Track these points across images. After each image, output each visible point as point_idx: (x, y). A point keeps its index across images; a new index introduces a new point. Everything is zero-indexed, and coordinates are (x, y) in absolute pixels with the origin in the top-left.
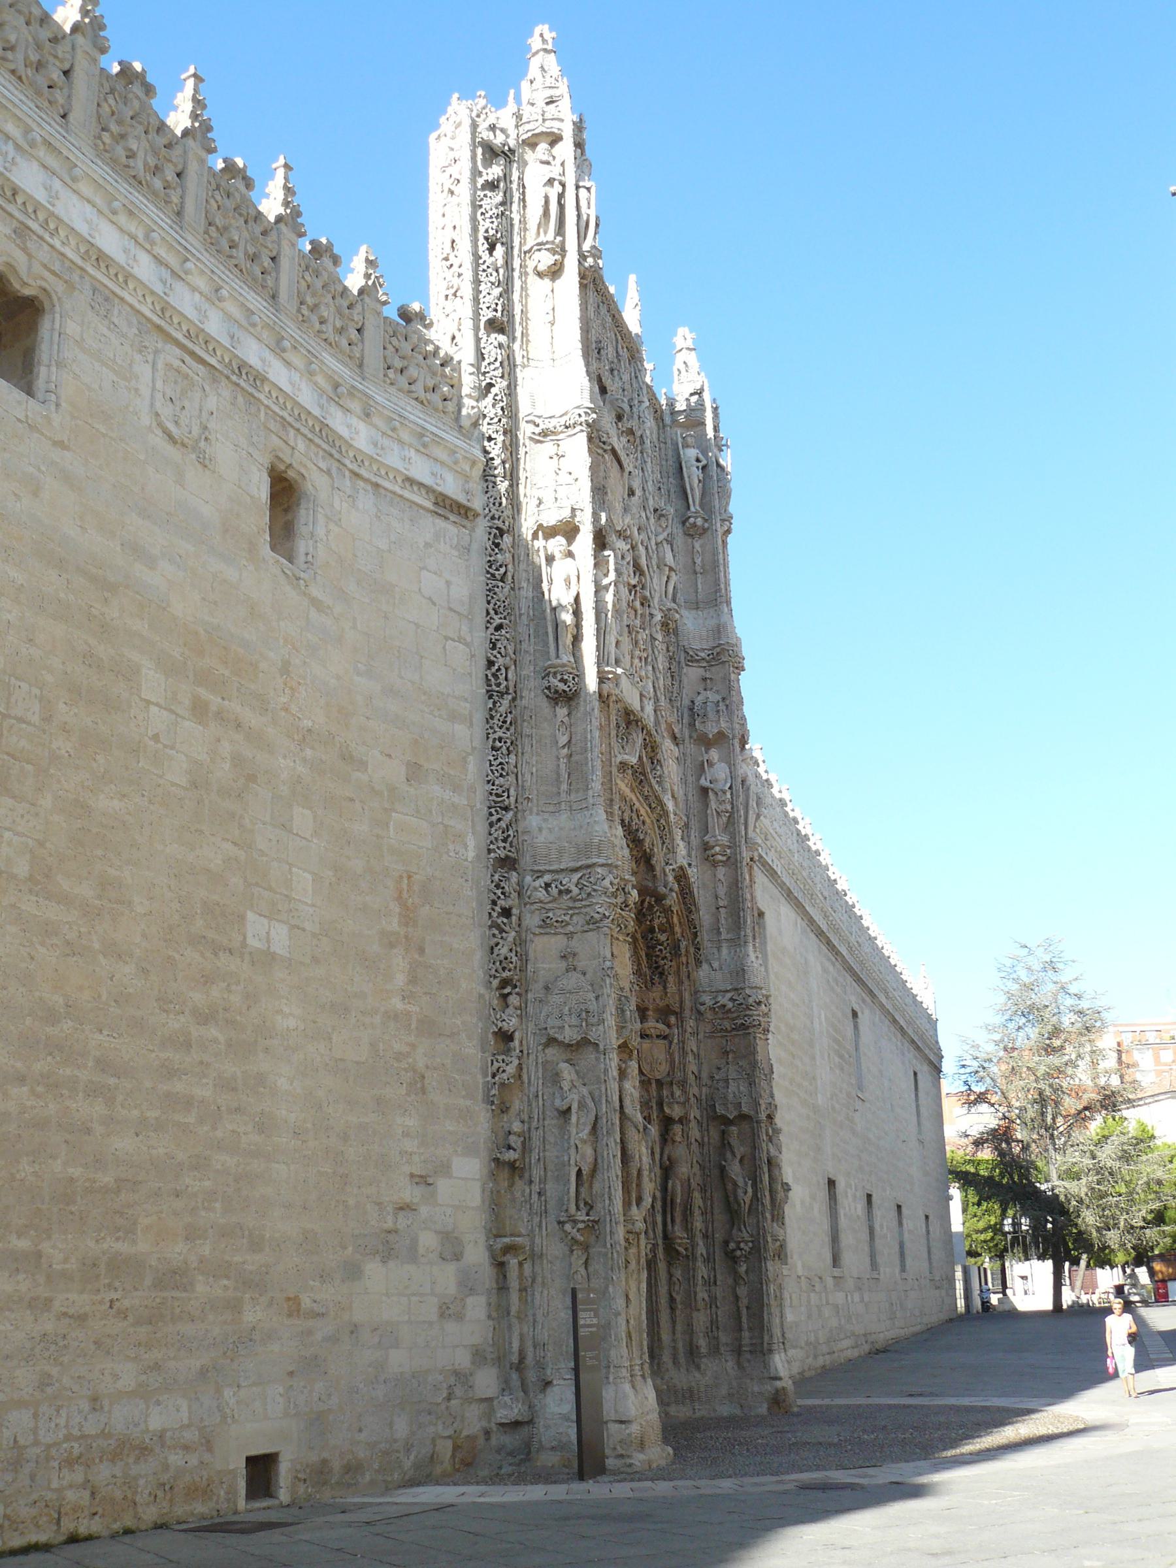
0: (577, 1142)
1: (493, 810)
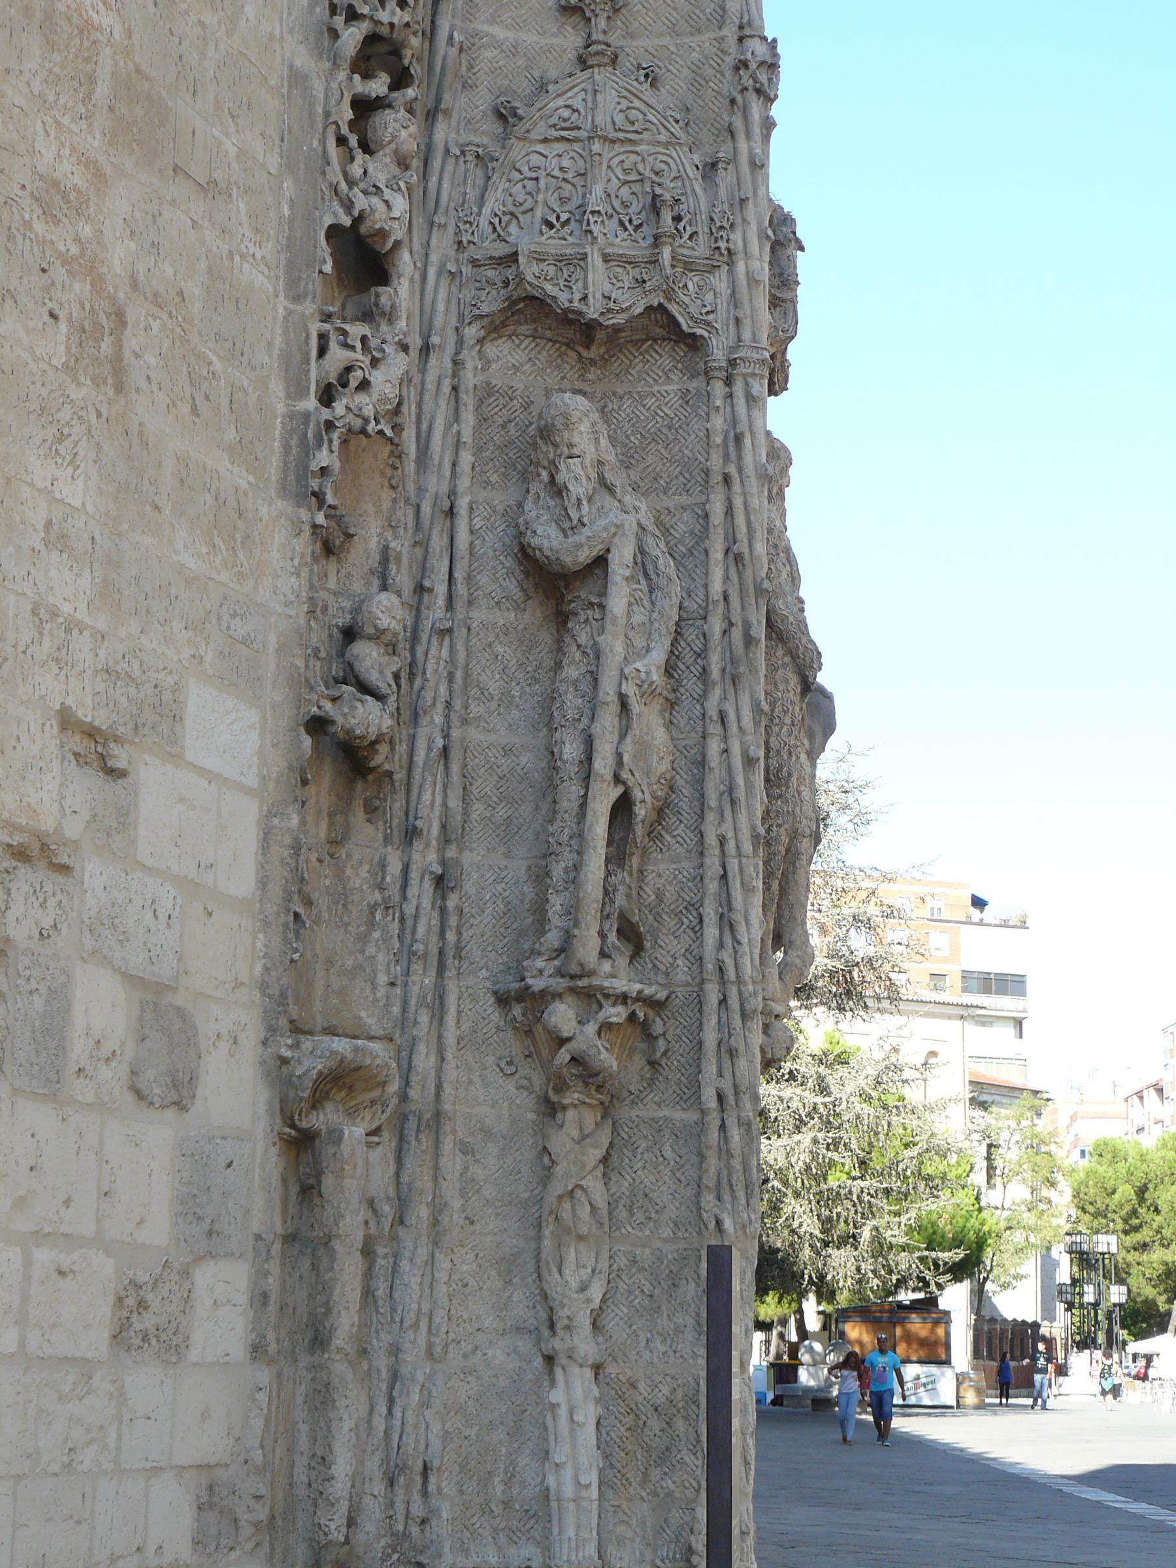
0: (630, 689)
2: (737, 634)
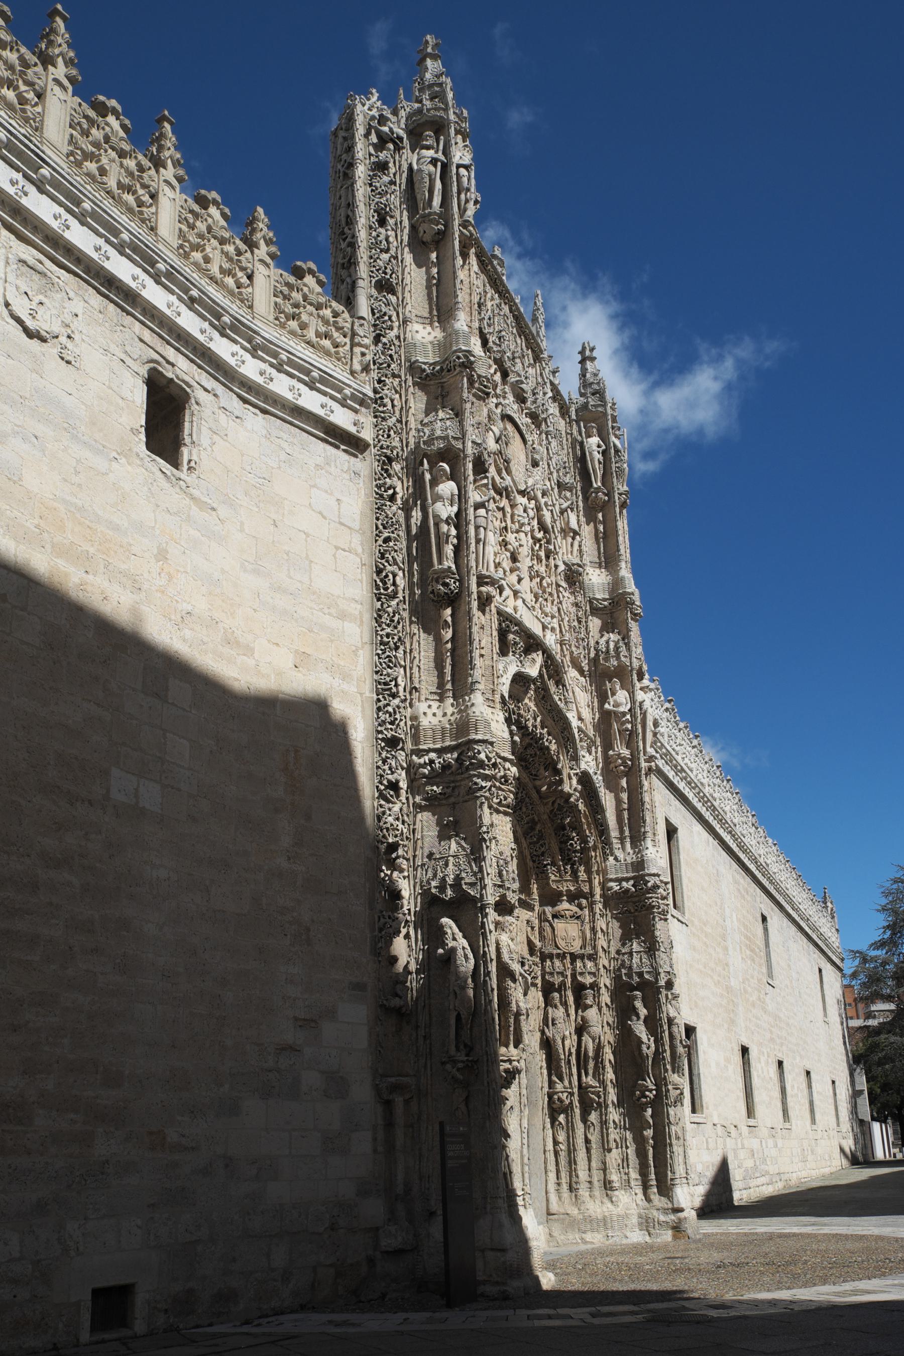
0: (456, 989)
1: (380, 697)
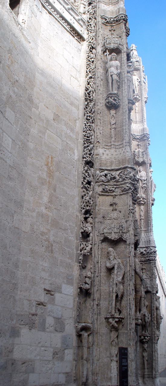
1: (86, 142)
2: (131, 275)
